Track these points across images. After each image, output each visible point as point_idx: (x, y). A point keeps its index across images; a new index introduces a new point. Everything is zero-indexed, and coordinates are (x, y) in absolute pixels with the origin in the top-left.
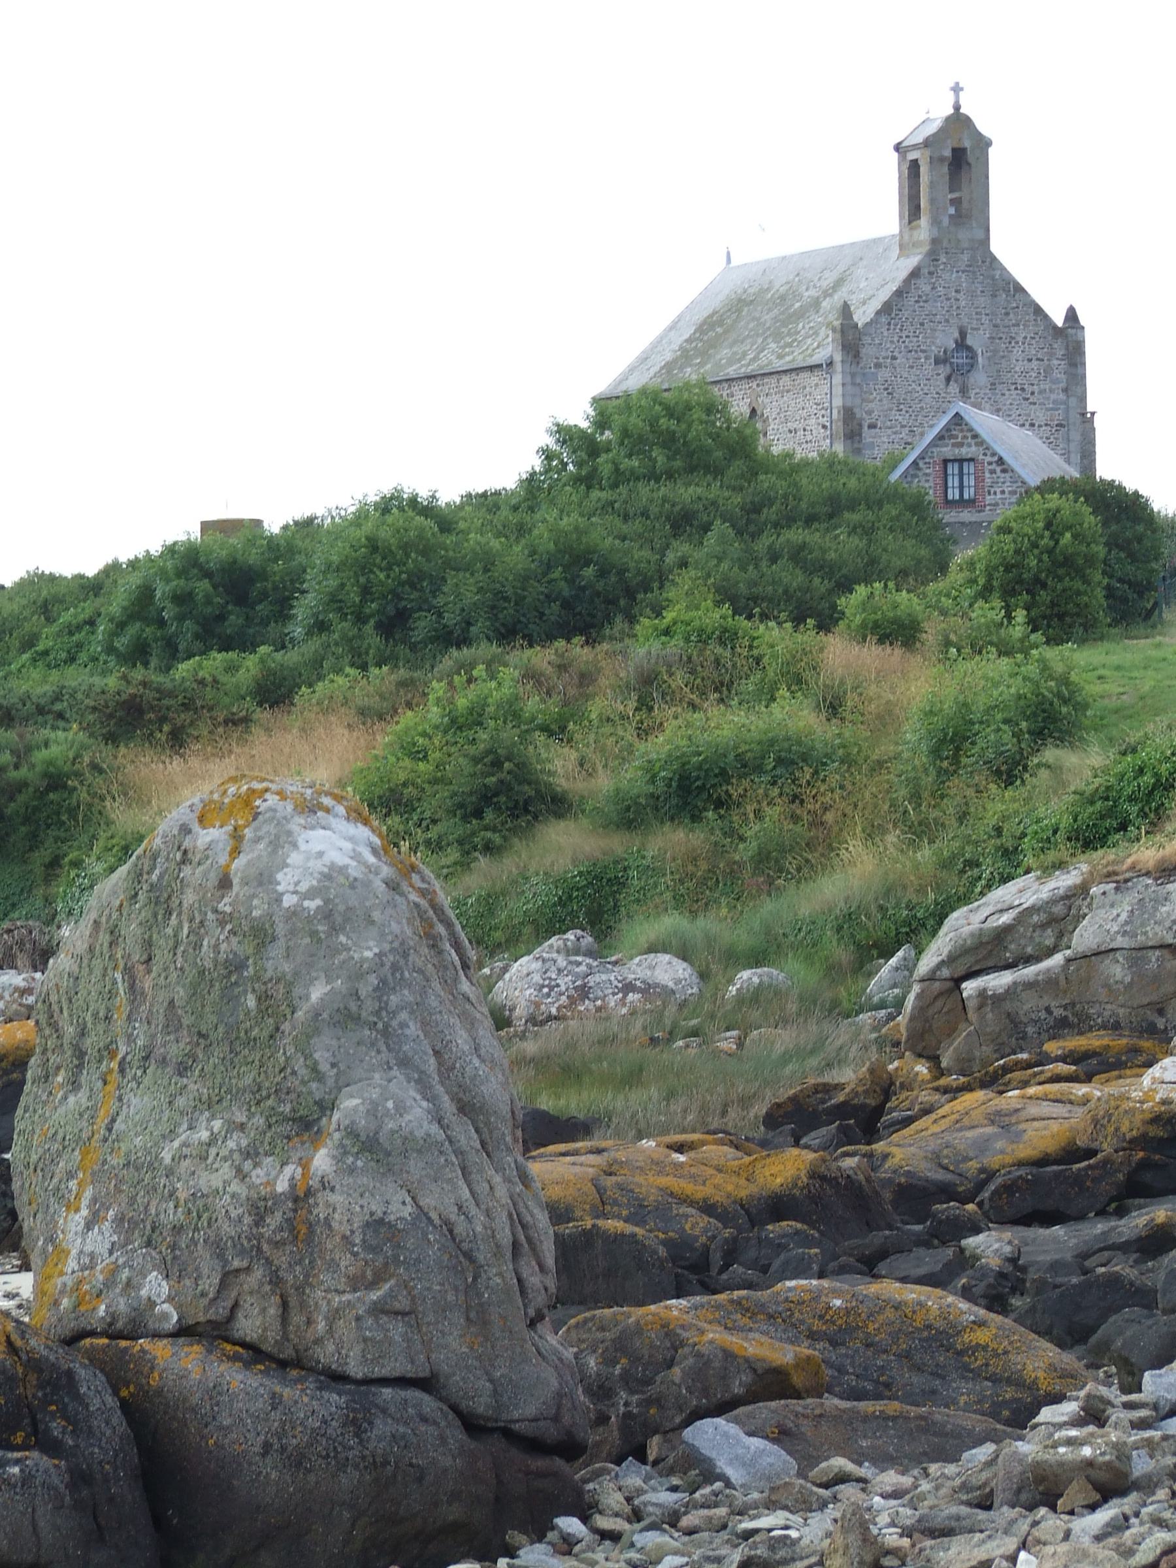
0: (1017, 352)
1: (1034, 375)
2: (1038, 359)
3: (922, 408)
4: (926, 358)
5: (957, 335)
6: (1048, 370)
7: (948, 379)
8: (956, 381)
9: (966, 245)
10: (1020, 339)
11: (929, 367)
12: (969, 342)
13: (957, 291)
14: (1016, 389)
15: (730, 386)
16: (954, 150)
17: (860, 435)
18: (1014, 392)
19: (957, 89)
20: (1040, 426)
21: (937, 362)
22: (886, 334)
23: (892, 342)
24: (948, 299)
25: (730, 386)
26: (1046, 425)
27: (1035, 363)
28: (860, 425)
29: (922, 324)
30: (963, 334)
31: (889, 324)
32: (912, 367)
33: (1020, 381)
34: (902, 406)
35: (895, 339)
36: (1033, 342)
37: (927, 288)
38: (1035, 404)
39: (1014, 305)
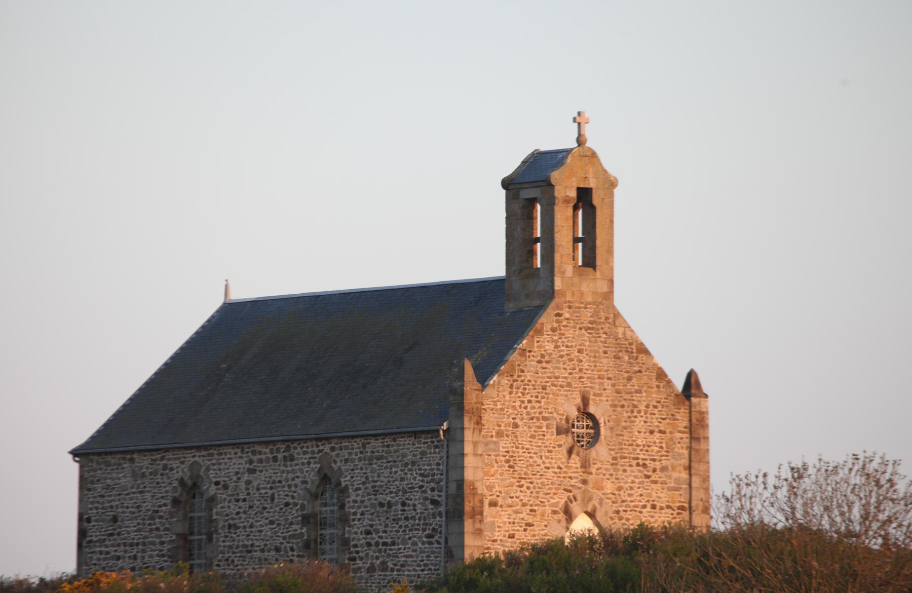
0: (639, 422)
1: (656, 449)
2: (660, 432)
3: (543, 483)
4: (548, 427)
5: (579, 401)
6: (671, 443)
7: (570, 452)
8: (578, 454)
9: (589, 299)
10: (643, 408)
11: (551, 437)
12: (592, 409)
13: (580, 351)
14: (638, 465)
15: (288, 449)
16: (579, 190)
17: (481, 513)
18: (635, 468)
19: (579, 121)
20: (662, 508)
21: (559, 432)
22: (507, 398)
23: (514, 407)
24: (571, 360)
25: (288, 449)
26: (668, 507)
27: (657, 435)
28: (481, 502)
29: (544, 388)
30: (585, 401)
31: (511, 387)
32: (533, 437)
33: (641, 456)
34: (523, 482)
35: (518, 404)
36: (656, 411)
37: (550, 347)
38: (655, 482)
39: (637, 369)
